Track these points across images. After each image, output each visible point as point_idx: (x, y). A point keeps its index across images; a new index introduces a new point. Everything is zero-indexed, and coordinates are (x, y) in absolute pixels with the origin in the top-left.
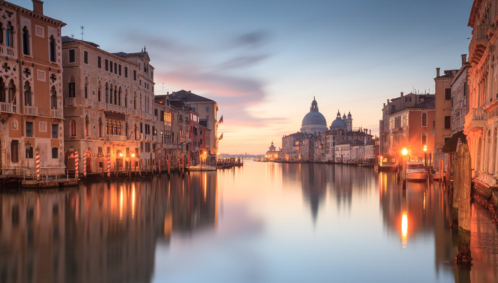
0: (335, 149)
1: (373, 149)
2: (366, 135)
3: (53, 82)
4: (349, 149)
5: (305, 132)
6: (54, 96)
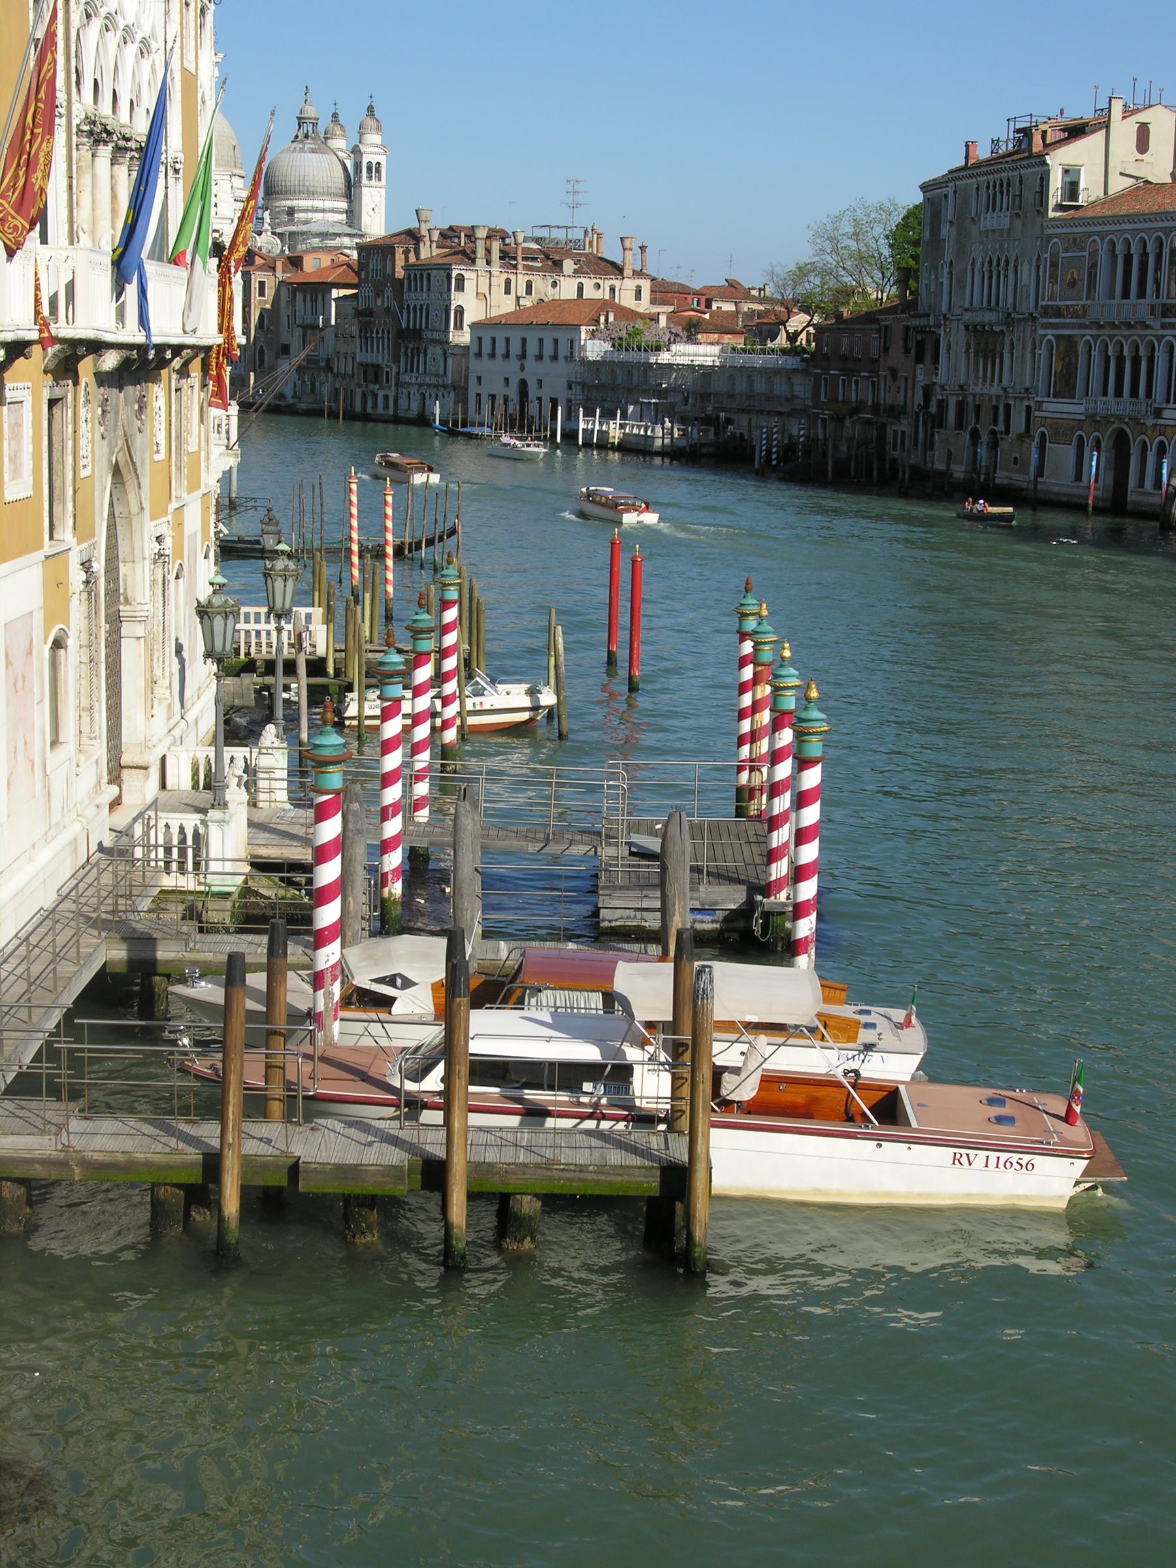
2: (628, 272)
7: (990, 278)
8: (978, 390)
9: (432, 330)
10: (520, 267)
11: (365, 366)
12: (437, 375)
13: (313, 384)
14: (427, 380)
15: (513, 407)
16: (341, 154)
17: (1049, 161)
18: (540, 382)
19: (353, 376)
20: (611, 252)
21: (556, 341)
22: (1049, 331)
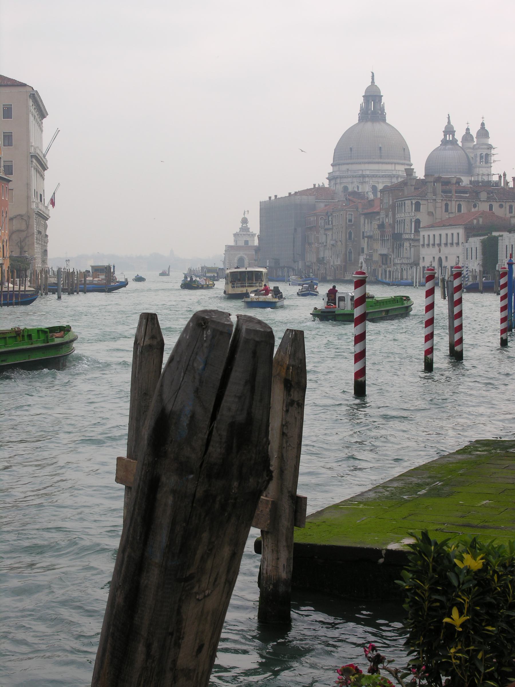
0: (421, 242)
4: (460, 242)
5: (343, 185)
9: (406, 233)
10: (454, 197)
11: (381, 255)
12: (407, 258)
13: (371, 268)
14: (404, 262)
16: (467, 151)
18: (447, 257)
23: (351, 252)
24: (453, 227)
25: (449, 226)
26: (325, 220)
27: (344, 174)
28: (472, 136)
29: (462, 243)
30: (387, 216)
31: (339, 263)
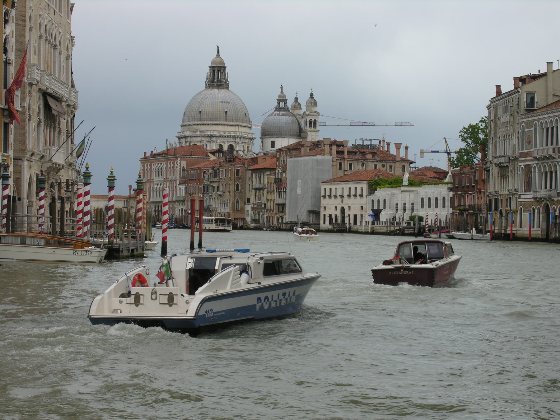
0: (323, 194)
1: (448, 194)
2: (398, 159)
3: (5, 27)
4: (365, 193)
6: (7, 63)
7: (505, 144)
8: (502, 193)
11: (278, 205)
13: (259, 215)
15: (340, 221)
16: (298, 117)
17: (520, 91)
18: (350, 207)
19: (274, 210)
20: (393, 151)
21: (356, 188)
22: (522, 164)
23: (238, 202)
24: (357, 182)
25: (352, 181)
26: (211, 173)
27: (194, 134)
28: (299, 104)
29: (366, 196)
30: (284, 171)
31: (228, 210)
